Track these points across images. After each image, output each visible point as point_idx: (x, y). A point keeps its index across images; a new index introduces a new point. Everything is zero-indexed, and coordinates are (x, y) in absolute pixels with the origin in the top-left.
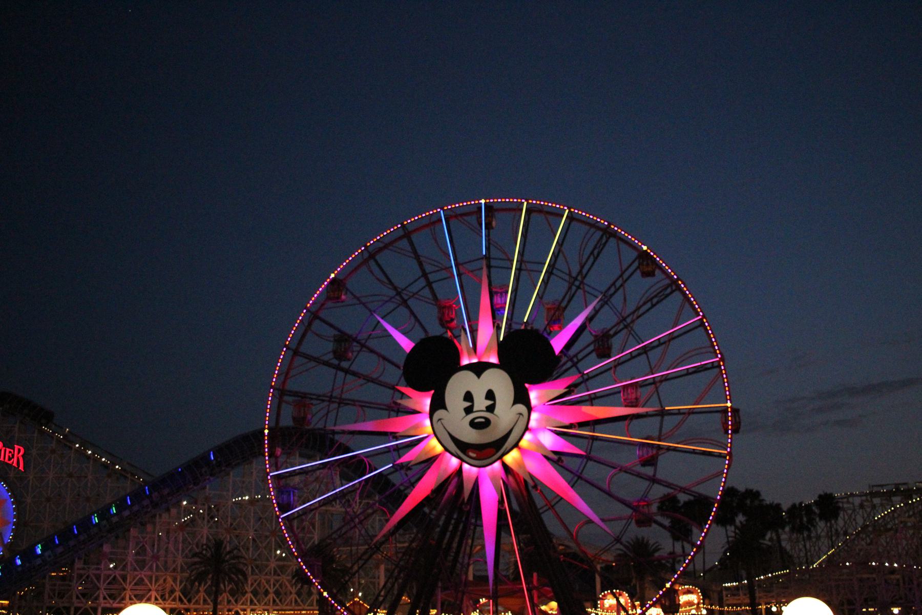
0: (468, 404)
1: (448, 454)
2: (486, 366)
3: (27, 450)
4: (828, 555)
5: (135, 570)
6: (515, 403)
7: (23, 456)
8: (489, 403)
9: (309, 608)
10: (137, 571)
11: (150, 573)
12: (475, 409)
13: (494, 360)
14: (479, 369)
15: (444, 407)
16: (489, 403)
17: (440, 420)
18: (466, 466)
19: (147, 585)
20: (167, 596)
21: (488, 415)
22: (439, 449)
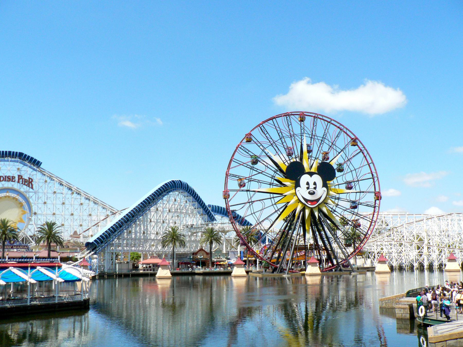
0: (308, 186)
8: (315, 186)
14: (311, 174)
15: (300, 187)
16: (315, 186)
18: (306, 207)
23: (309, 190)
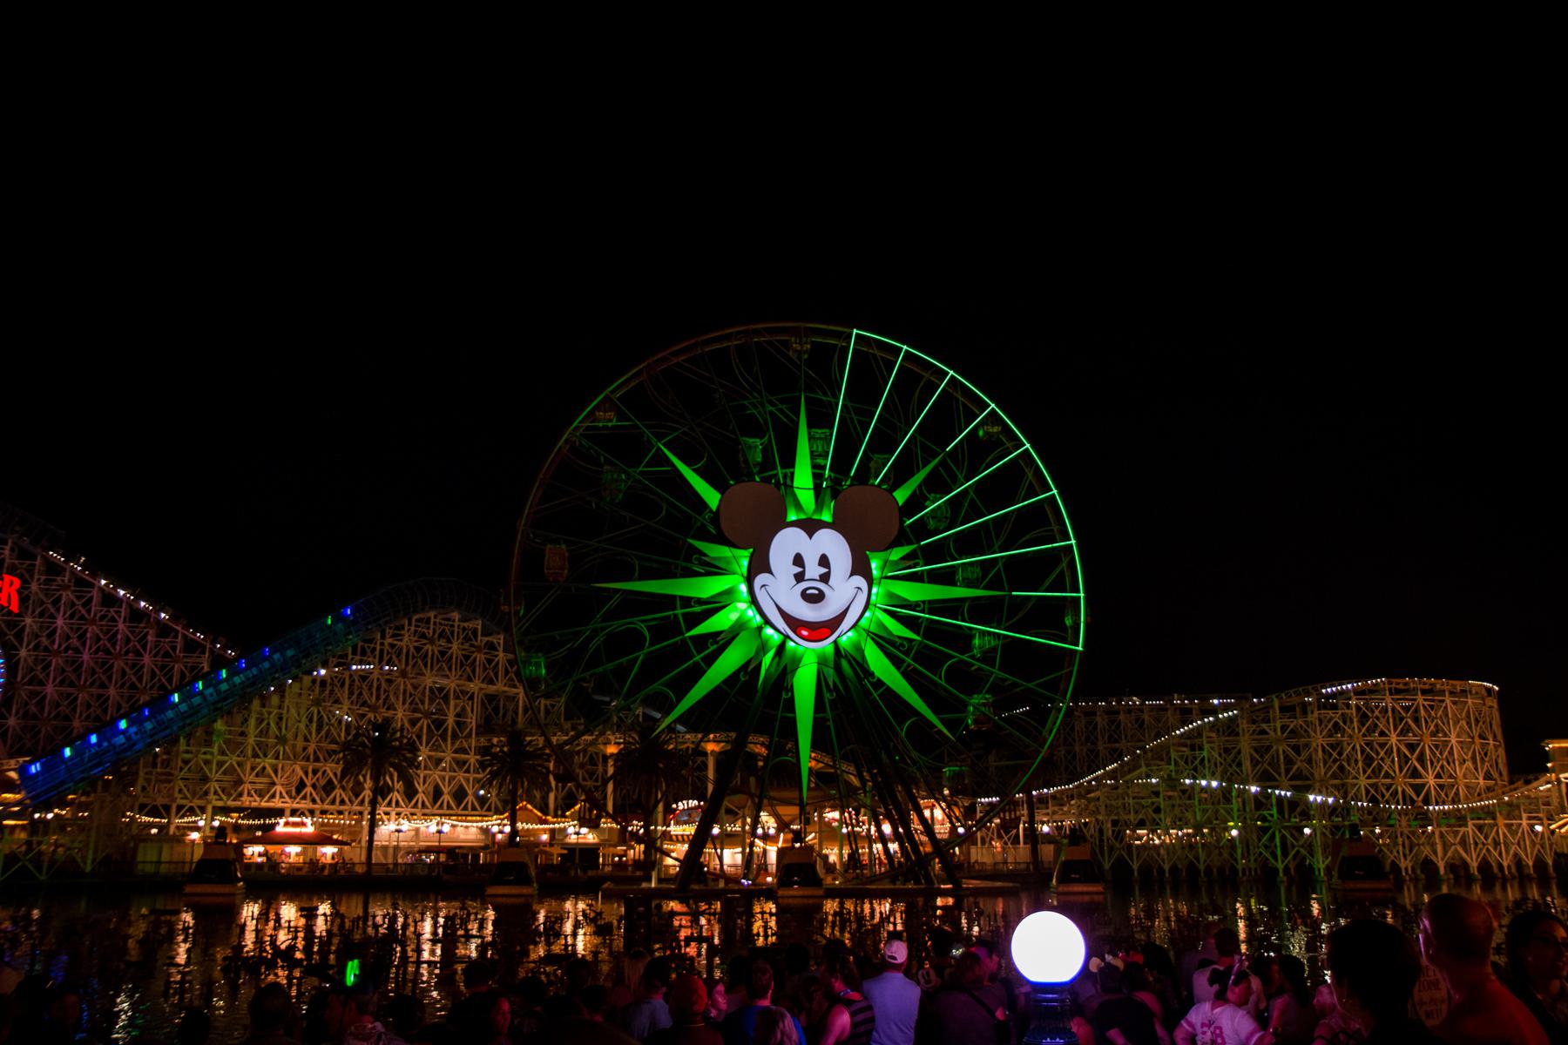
0: (800, 570)
1: (768, 631)
2: (822, 525)
3: (25, 583)
4: (1104, 769)
5: (255, 756)
6: (851, 575)
7: (17, 591)
8: (824, 570)
9: (466, 812)
10: (259, 757)
11: (274, 761)
12: (806, 578)
13: (827, 516)
14: (810, 526)
15: (770, 572)
16: (824, 570)
17: (764, 586)
18: (790, 644)
19: (270, 777)
20: (294, 793)
21: (822, 586)
22: (758, 620)
23: (804, 585)
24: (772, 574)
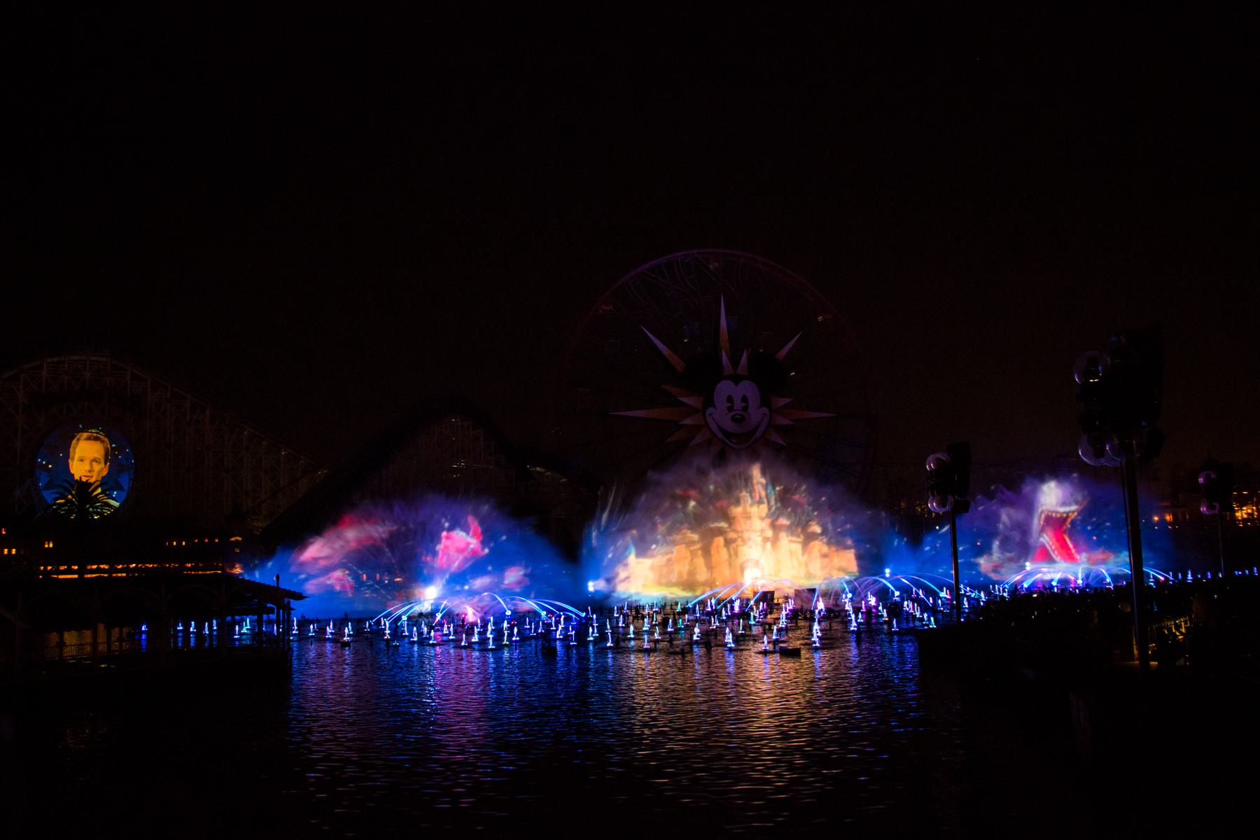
0: (729, 405)
6: (761, 406)
8: (744, 404)
14: (736, 379)
15: (714, 407)
16: (744, 404)
17: (711, 414)
21: (743, 413)
23: (732, 414)
24: (716, 408)
